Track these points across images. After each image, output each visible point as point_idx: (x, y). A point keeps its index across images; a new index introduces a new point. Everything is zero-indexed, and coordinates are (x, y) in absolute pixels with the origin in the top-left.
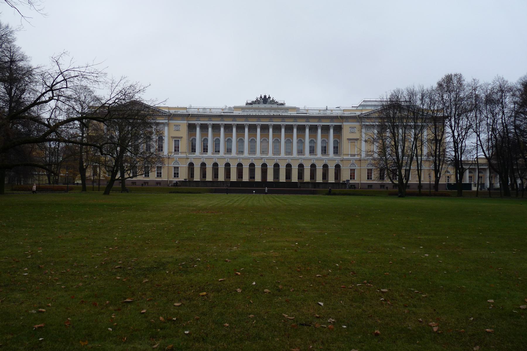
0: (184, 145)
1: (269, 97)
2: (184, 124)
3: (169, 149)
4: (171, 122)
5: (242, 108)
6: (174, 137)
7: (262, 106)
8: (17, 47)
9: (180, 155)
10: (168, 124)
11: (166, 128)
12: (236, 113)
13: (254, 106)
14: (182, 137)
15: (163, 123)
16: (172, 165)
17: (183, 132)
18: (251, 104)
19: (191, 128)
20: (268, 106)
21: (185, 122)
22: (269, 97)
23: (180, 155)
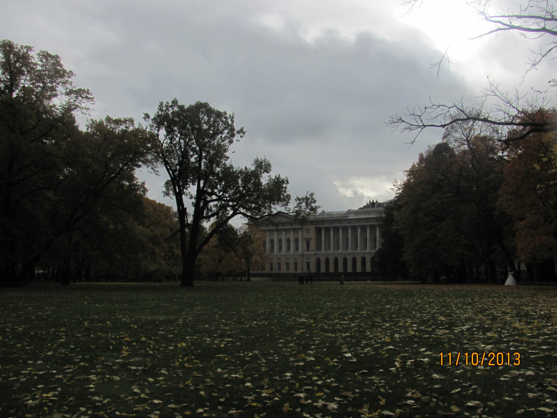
0: (313, 244)
1: (377, 202)
2: (312, 228)
3: (302, 248)
4: (304, 226)
5: (356, 212)
6: (305, 239)
7: (370, 209)
8: (244, 168)
9: (310, 253)
10: (301, 229)
11: (300, 232)
12: (351, 217)
13: (364, 210)
14: (311, 239)
15: (297, 228)
16: (305, 260)
17: (312, 235)
18: (362, 208)
19: (319, 230)
20: (374, 209)
21: (313, 226)
22: (377, 202)
23: (310, 253)
